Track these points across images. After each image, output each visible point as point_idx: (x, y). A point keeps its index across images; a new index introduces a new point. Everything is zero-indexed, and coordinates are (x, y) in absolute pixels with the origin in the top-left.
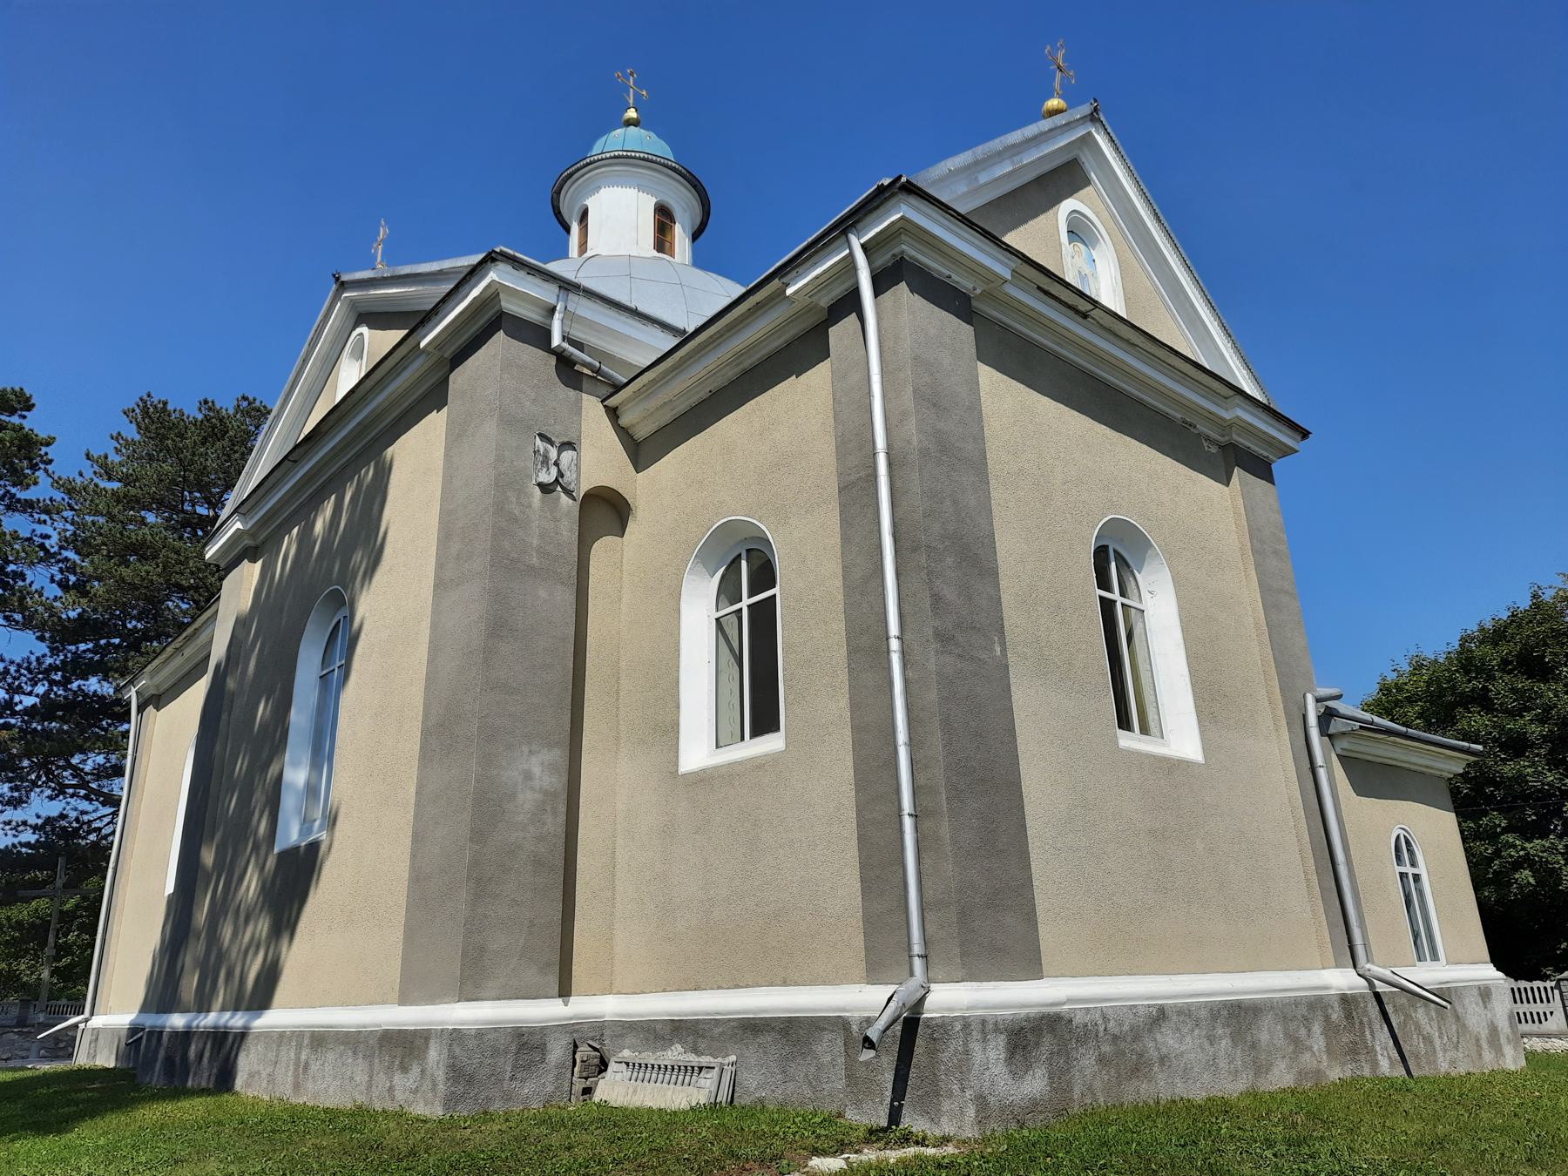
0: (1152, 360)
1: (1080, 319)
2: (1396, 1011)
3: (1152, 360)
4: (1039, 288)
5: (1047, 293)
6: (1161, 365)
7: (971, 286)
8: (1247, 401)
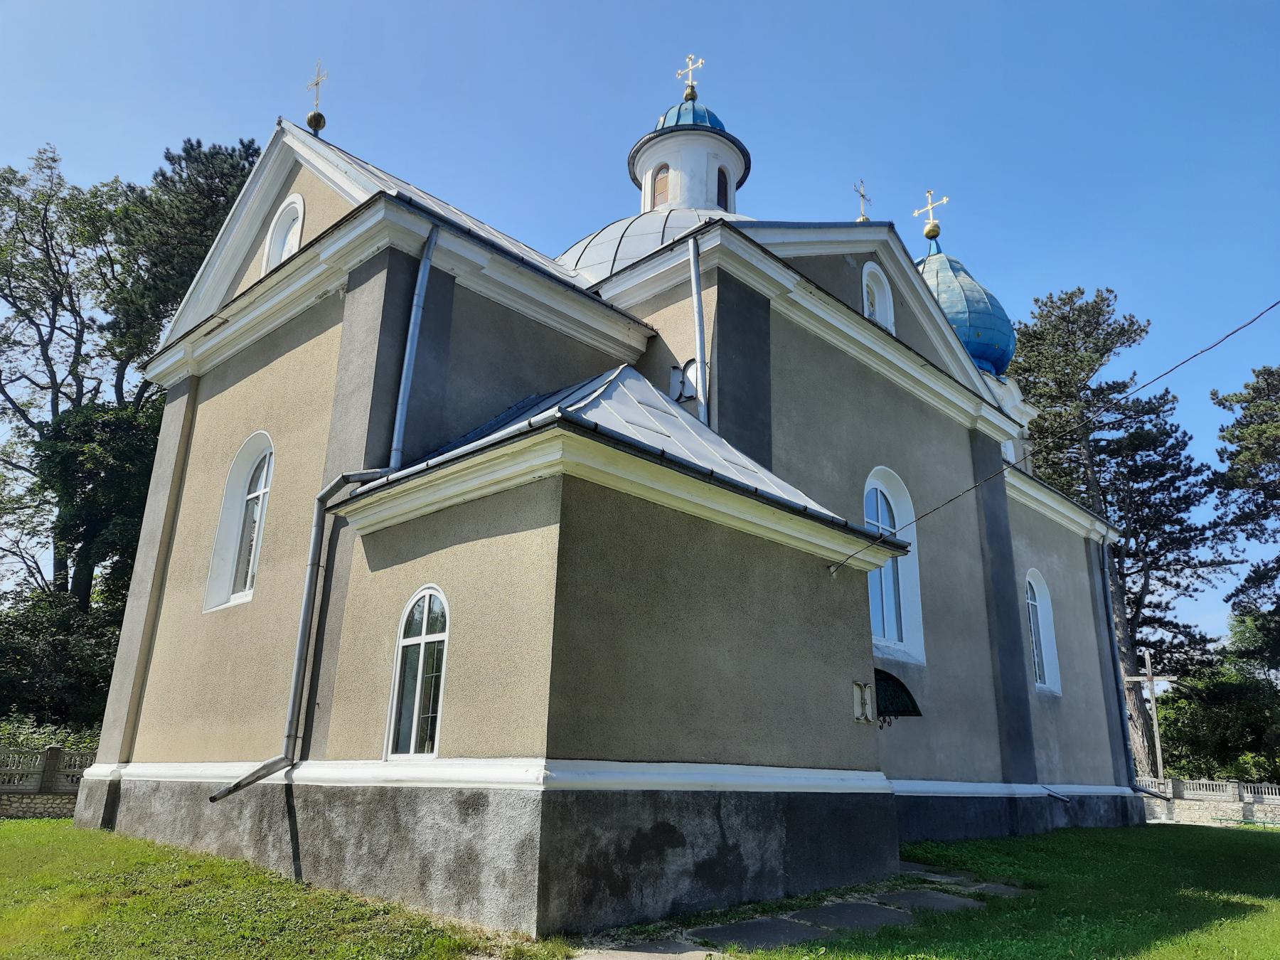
0: (267, 295)
1: (227, 325)
2: (305, 807)
3: (267, 295)
4: (205, 335)
5: (209, 333)
6: (274, 290)
7: (186, 372)
8: (323, 241)
